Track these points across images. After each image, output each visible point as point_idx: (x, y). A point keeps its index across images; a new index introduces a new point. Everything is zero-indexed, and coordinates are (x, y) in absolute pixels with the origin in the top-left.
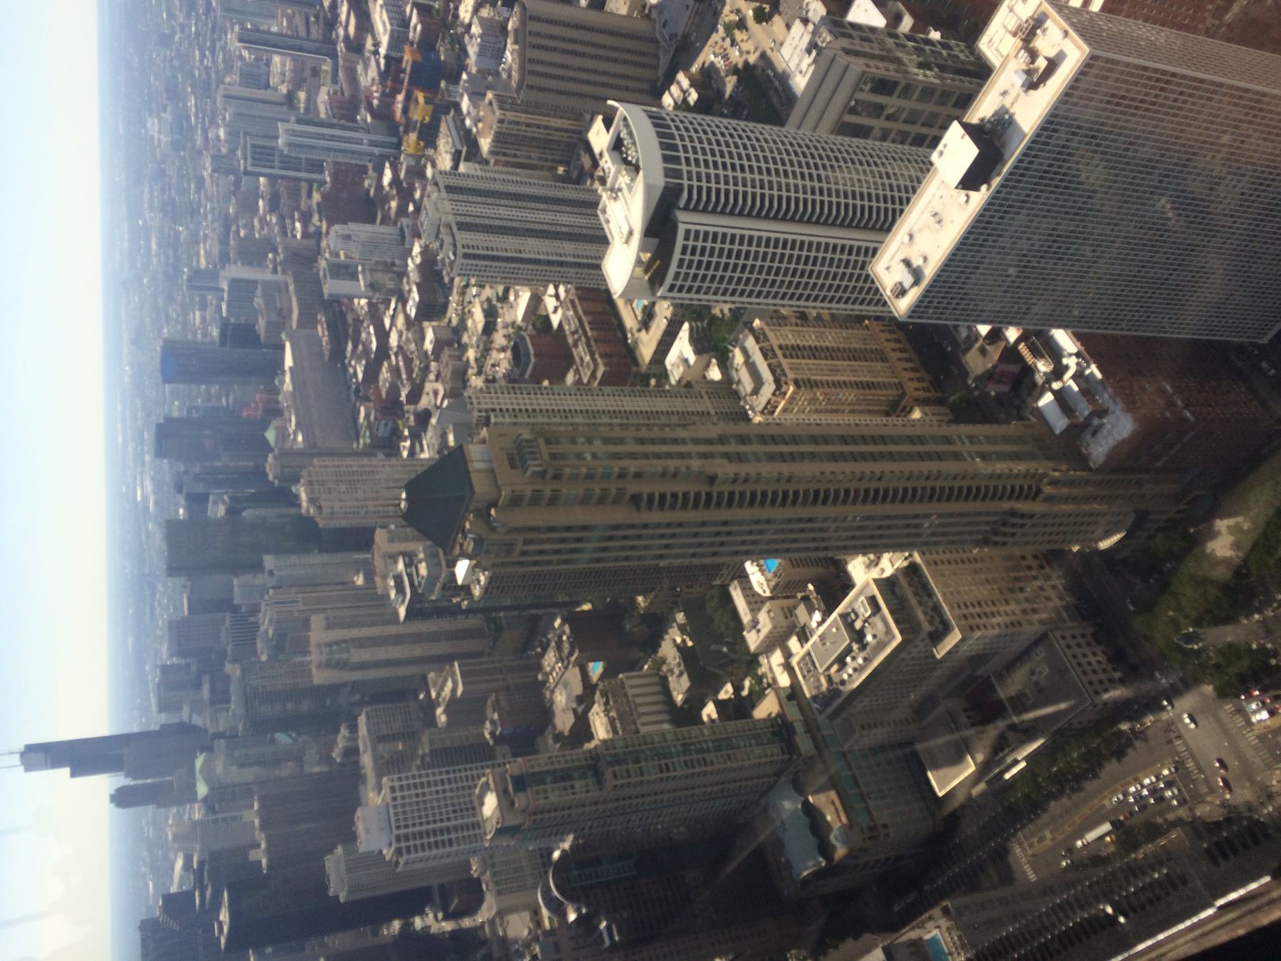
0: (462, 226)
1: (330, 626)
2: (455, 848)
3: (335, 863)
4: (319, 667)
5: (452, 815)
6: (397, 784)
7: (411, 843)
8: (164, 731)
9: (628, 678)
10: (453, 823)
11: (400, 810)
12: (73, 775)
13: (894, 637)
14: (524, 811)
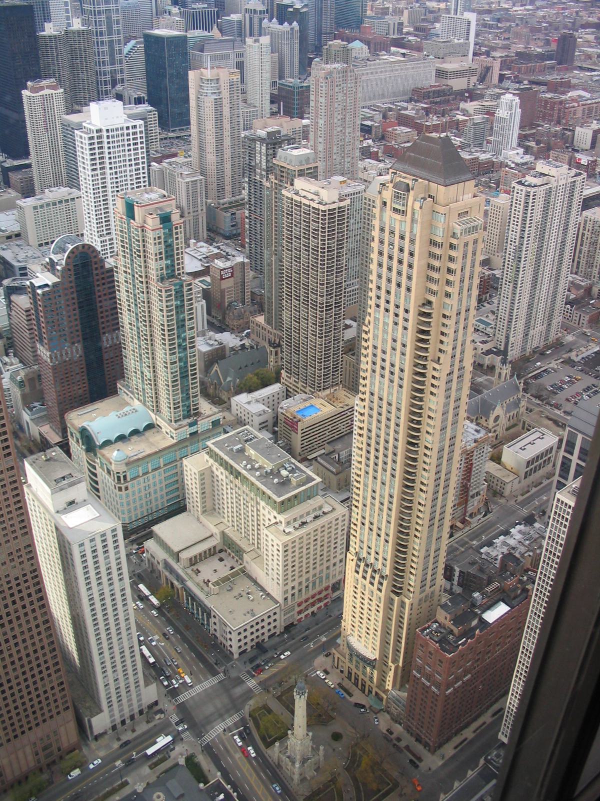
0: (549, 193)
5: (114, 171)
6: (138, 130)
9: (202, 306)
10: (108, 171)
13: (280, 496)
14: (145, 222)
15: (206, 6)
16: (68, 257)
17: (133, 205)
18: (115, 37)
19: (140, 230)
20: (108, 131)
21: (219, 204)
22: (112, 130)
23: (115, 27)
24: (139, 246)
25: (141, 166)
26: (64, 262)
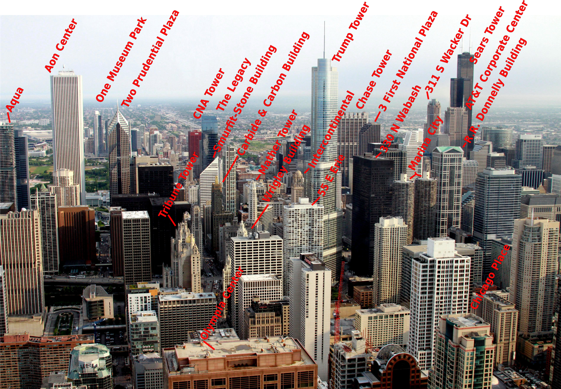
1: (551, 233)
2: (420, 295)
3: (396, 222)
4: (525, 222)
5: (440, 296)
6: (465, 264)
7: (428, 269)
8: (471, 131)
10: (436, 296)
11: (450, 264)
12: (452, 80)
14: (461, 343)
15: (535, 167)
16: (390, 363)
17: (453, 327)
18: (455, 188)
19: (455, 349)
20: (439, 262)
21: (529, 336)
22: (444, 262)
23: (456, 180)
24: (453, 363)
25: (464, 294)
26: (385, 367)
